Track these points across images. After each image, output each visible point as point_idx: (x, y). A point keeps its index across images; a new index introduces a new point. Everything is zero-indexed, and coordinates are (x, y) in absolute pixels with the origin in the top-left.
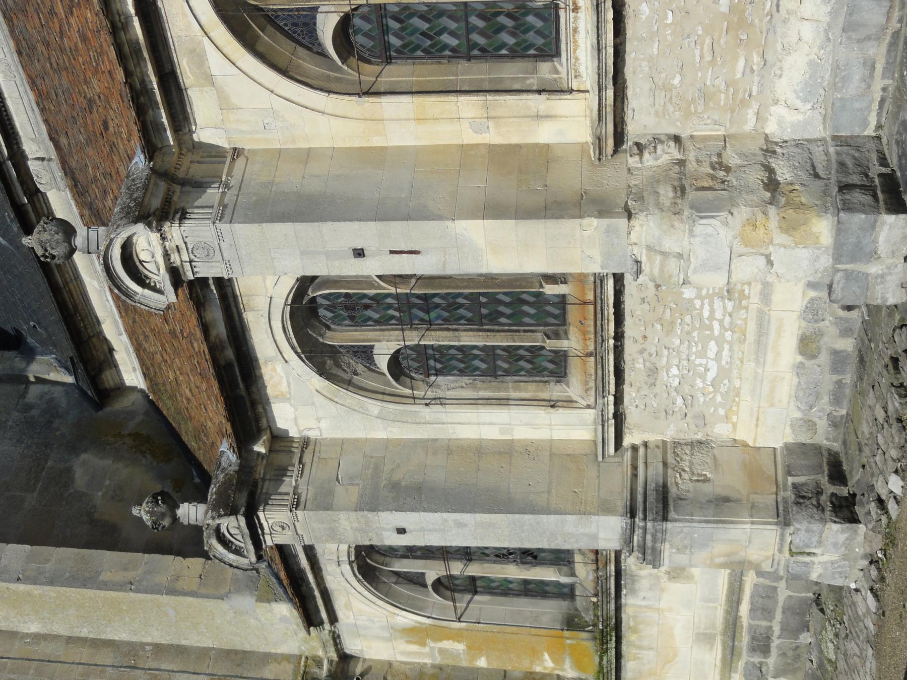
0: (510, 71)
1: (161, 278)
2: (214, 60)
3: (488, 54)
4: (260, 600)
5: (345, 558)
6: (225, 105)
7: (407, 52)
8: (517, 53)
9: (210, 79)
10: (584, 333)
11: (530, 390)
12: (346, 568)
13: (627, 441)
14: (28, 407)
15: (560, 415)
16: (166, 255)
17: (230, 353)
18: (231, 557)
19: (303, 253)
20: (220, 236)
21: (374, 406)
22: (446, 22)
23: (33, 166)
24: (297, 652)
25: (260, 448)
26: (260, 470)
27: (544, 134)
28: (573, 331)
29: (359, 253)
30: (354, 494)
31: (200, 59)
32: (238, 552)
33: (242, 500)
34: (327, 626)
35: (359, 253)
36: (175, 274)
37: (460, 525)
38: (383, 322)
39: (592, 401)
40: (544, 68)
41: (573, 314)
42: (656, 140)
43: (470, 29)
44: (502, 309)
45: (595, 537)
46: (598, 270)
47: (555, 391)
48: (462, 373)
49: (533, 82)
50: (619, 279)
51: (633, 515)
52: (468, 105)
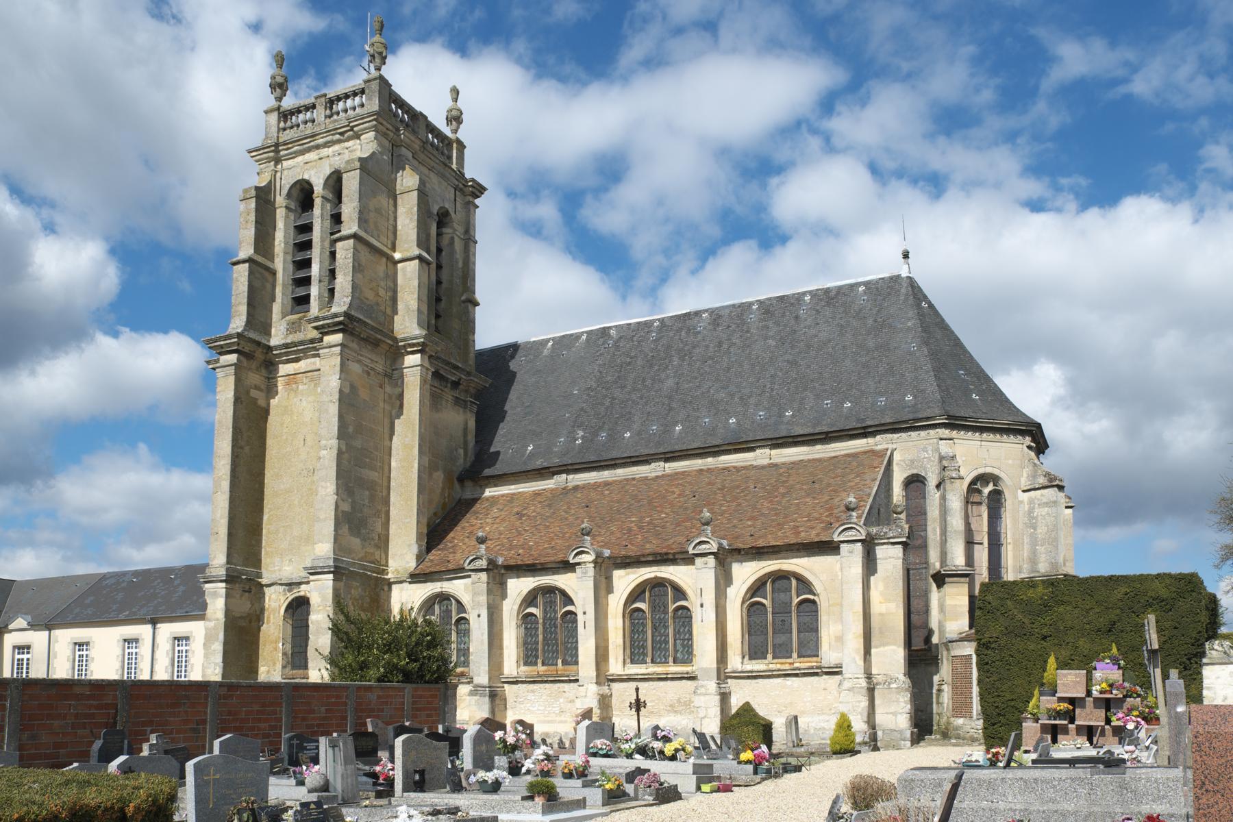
0: (628, 652)
1: (577, 560)
2: (632, 577)
3: (632, 646)
4: (417, 555)
5: (444, 590)
6: (622, 577)
7: (632, 624)
8: (632, 653)
9: (628, 574)
10: (546, 671)
11: (522, 655)
12: (439, 590)
13: (506, 685)
14: (456, 450)
15: (515, 664)
16: (585, 562)
17: (539, 567)
18: (468, 561)
19: (584, 598)
20: (589, 577)
21: (516, 607)
22: (641, 635)
23: (564, 476)
24: (389, 565)
25: (503, 571)
26: (495, 571)
27: (612, 660)
28: (545, 668)
29: (584, 613)
30: (491, 602)
31: (633, 573)
32: (469, 564)
33: (490, 567)
34: (409, 580)
35: (584, 613)
36: (579, 564)
37: (482, 634)
38: (545, 612)
39: (520, 673)
40: (628, 660)
41: (554, 667)
42: (611, 689)
43: (639, 642)
44: (551, 647)
45: (479, 676)
46: (580, 674)
47: (522, 663)
48: (526, 634)
49: (626, 657)
50: (577, 681)
51: (489, 687)
52: (620, 641)
